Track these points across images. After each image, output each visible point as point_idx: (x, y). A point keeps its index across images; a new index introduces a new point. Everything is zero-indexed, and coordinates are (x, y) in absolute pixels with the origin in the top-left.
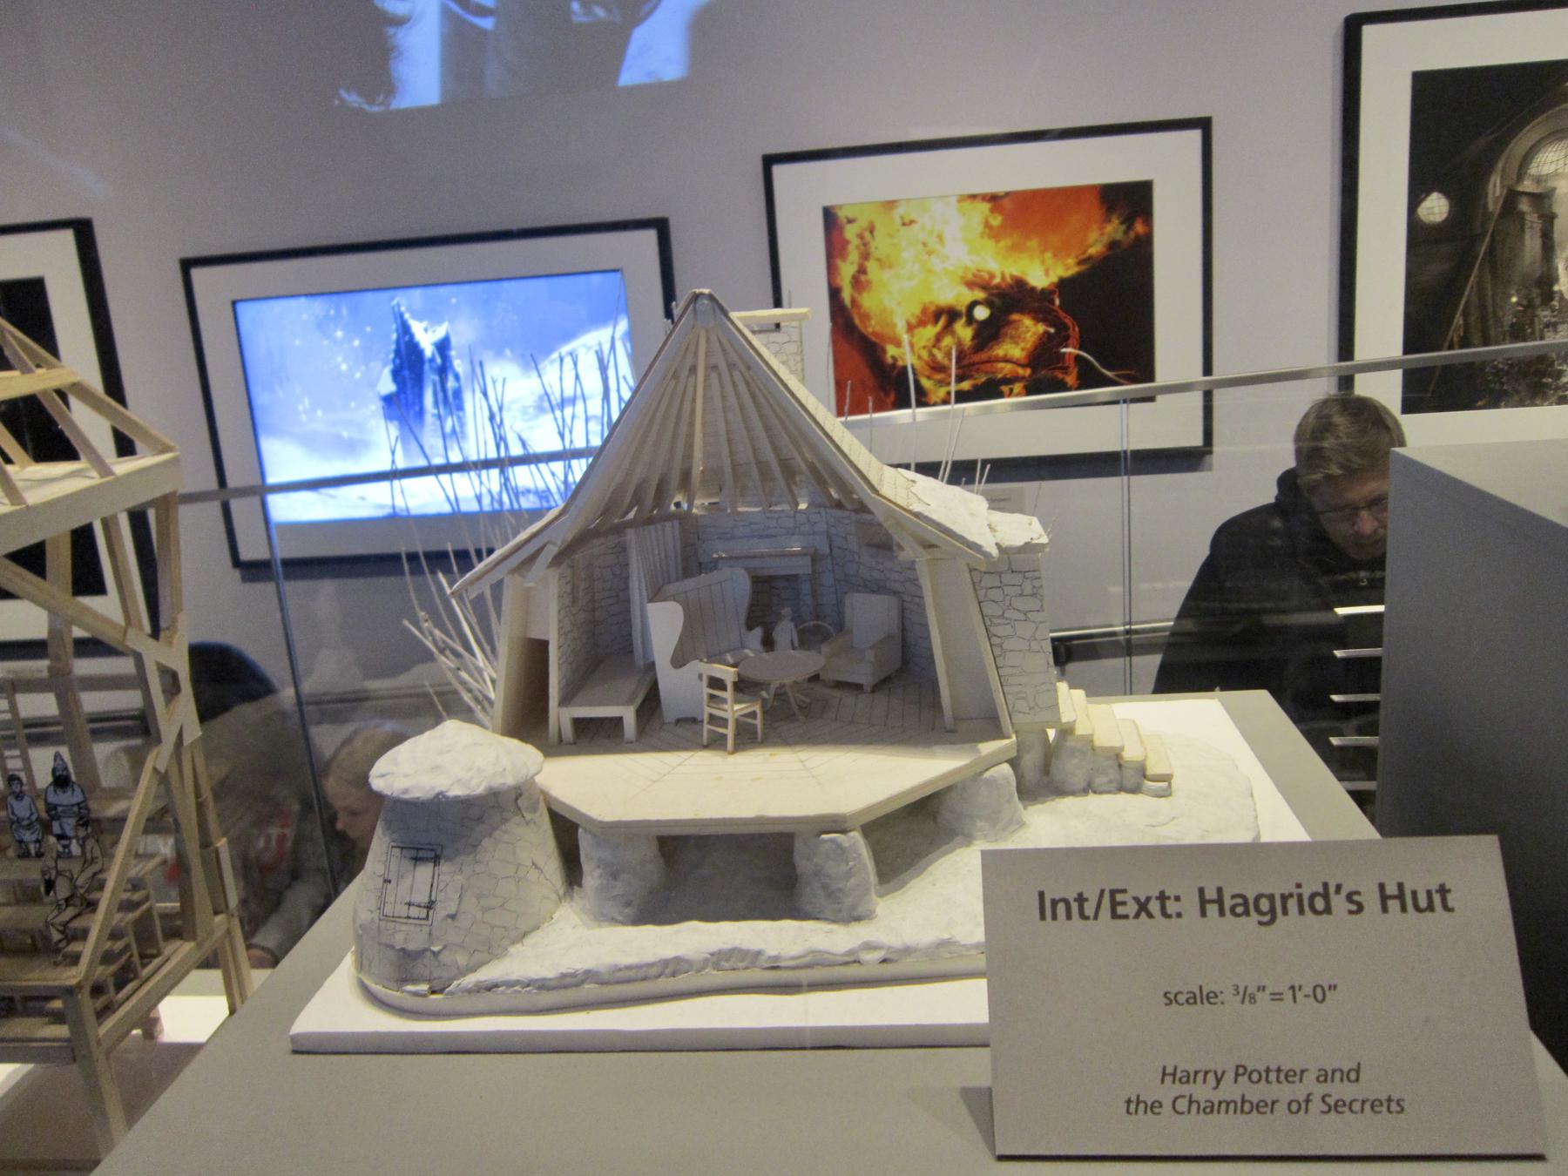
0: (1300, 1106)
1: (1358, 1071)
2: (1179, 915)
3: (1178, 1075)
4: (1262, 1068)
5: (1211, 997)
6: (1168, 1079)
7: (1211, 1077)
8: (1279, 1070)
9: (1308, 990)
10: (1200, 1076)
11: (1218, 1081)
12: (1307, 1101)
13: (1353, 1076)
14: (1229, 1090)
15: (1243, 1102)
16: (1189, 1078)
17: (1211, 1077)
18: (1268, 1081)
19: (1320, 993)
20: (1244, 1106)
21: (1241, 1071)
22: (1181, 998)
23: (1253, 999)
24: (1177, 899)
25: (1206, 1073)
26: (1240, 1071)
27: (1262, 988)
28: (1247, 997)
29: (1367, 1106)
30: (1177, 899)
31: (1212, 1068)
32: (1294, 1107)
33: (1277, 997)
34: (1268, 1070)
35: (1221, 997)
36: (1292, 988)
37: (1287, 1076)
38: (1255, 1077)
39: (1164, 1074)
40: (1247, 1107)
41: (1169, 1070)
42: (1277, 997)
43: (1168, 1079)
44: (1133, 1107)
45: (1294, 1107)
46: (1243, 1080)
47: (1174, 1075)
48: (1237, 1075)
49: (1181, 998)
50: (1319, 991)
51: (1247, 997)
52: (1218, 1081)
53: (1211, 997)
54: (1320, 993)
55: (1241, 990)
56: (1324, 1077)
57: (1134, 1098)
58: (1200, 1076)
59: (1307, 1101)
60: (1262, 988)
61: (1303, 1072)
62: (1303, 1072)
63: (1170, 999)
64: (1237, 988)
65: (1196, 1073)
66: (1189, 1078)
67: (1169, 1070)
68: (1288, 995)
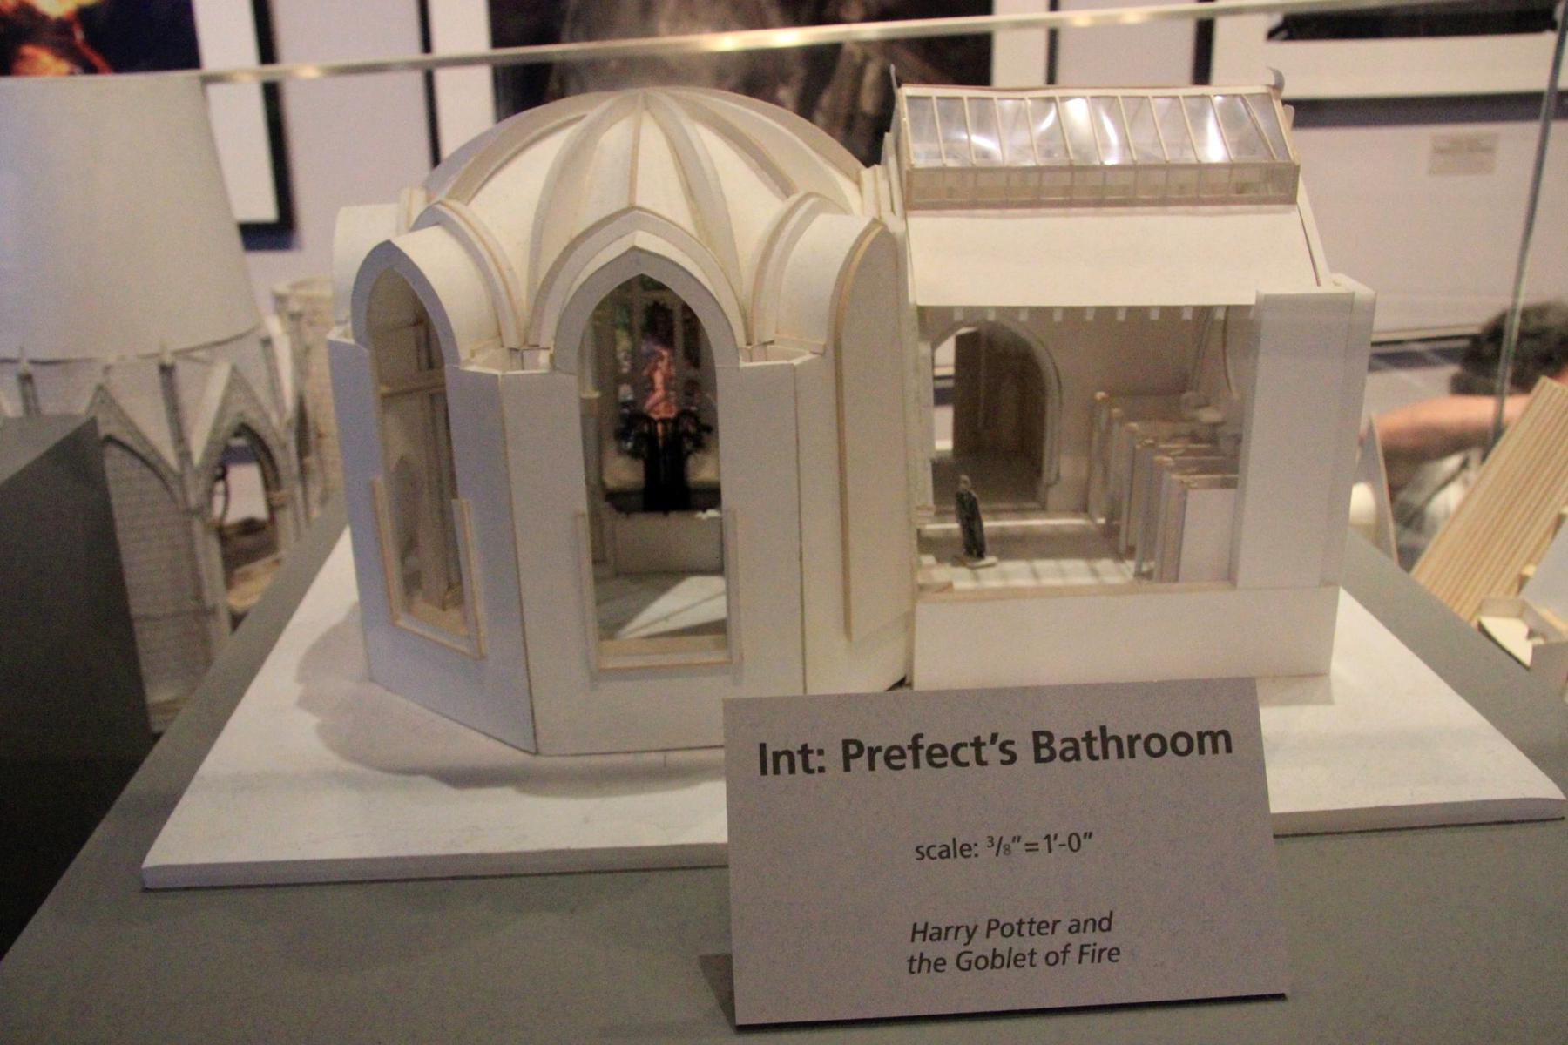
0: (1057, 958)
1: (1110, 920)
2: (821, 770)
3: (930, 931)
4: (1015, 921)
5: (965, 850)
6: (919, 937)
7: (963, 934)
8: (1031, 922)
9: (1063, 839)
10: (952, 932)
11: (970, 937)
12: (1065, 952)
13: (1105, 924)
14: (982, 946)
15: (994, 956)
16: (938, 935)
17: (963, 934)
18: (1020, 934)
19: (1075, 842)
20: (994, 961)
21: (994, 924)
22: (934, 852)
23: (1008, 850)
24: (821, 752)
25: (958, 928)
26: (993, 925)
27: (1017, 839)
28: (1001, 847)
29: (1105, 954)
30: (821, 752)
31: (966, 922)
32: (1052, 959)
33: (1032, 847)
34: (1021, 923)
35: (975, 850)
36: (1048, 837)
37: (1039, 929)
38: (1007, 930)
39: (915, 932)
40: (998, 962)
41: (920, 927)
42: (1032, 847)
43: (919, 937)
44: (915, 965)
45: (1052, 959)
47: (924, 932)
48: (989, 929)
49: (934, 852)
50: (1074, 838)
51: (1001, 847)
52: (970, 937)
53: (965, 850)
54: (1075, 842)
55: (996, 841)
56: (1076, 927)
57: (917, 957)
58: (952, 932)
59: (1065, 952)
60: (1017, 839)
61: (1055, 923)
62: (1055, 923)
63: (922, 853)
64: (992, 841)
65: (948, 929)
66: (938, 935)
67: (920, 927)
68: (1043, 845)
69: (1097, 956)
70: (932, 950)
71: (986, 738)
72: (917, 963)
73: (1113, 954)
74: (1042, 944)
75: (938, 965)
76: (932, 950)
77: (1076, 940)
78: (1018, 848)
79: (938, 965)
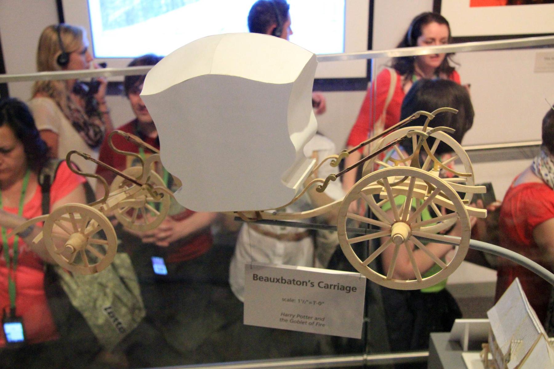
4: (303, 315)
9: (317, 302)
16: (287, 315)
19: (320, 303)
27: (307, 301)
33: (310, 303)
42: (310, 303)
46: (299, 317)
54: (320, 303)
56: (316, 319)
60: (307, 301)
66: (287, 315)
69: (320, 325)
70: (285, 318)
71: (307, 281)
72: (282, 320)
73: (323, 325)
74: (308, 321)
75: (286, 321)
76: (285, 318)
77: (316, 322)
78: (307, 303)
79: (286, 321)
